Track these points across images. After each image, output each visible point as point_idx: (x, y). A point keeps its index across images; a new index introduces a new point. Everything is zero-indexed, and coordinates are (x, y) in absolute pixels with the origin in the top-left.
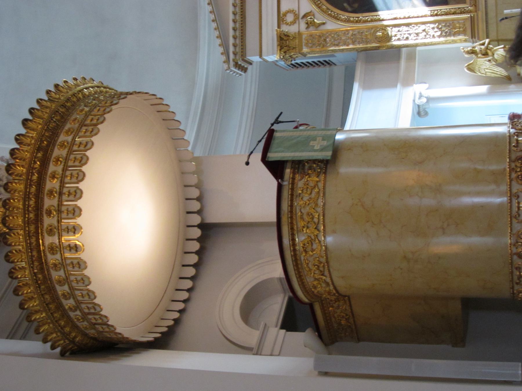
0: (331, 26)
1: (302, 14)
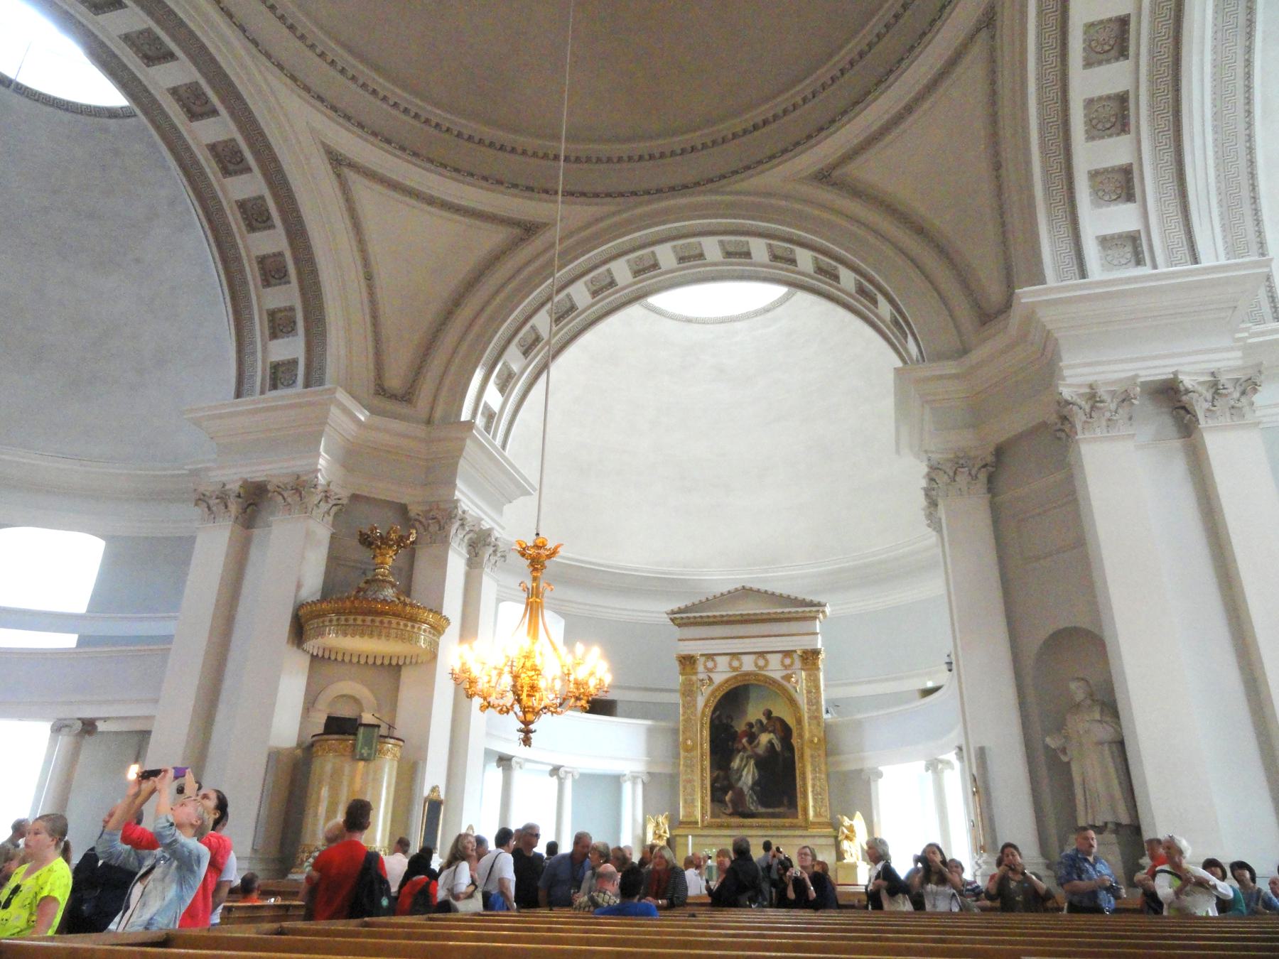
0: (701, 701)
1: (710, 674)
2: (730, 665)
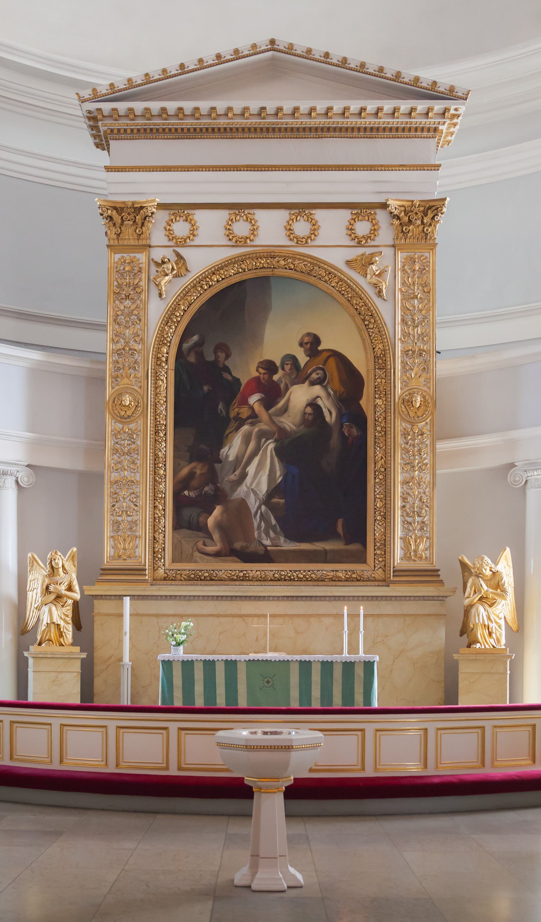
2: (229, 233)
